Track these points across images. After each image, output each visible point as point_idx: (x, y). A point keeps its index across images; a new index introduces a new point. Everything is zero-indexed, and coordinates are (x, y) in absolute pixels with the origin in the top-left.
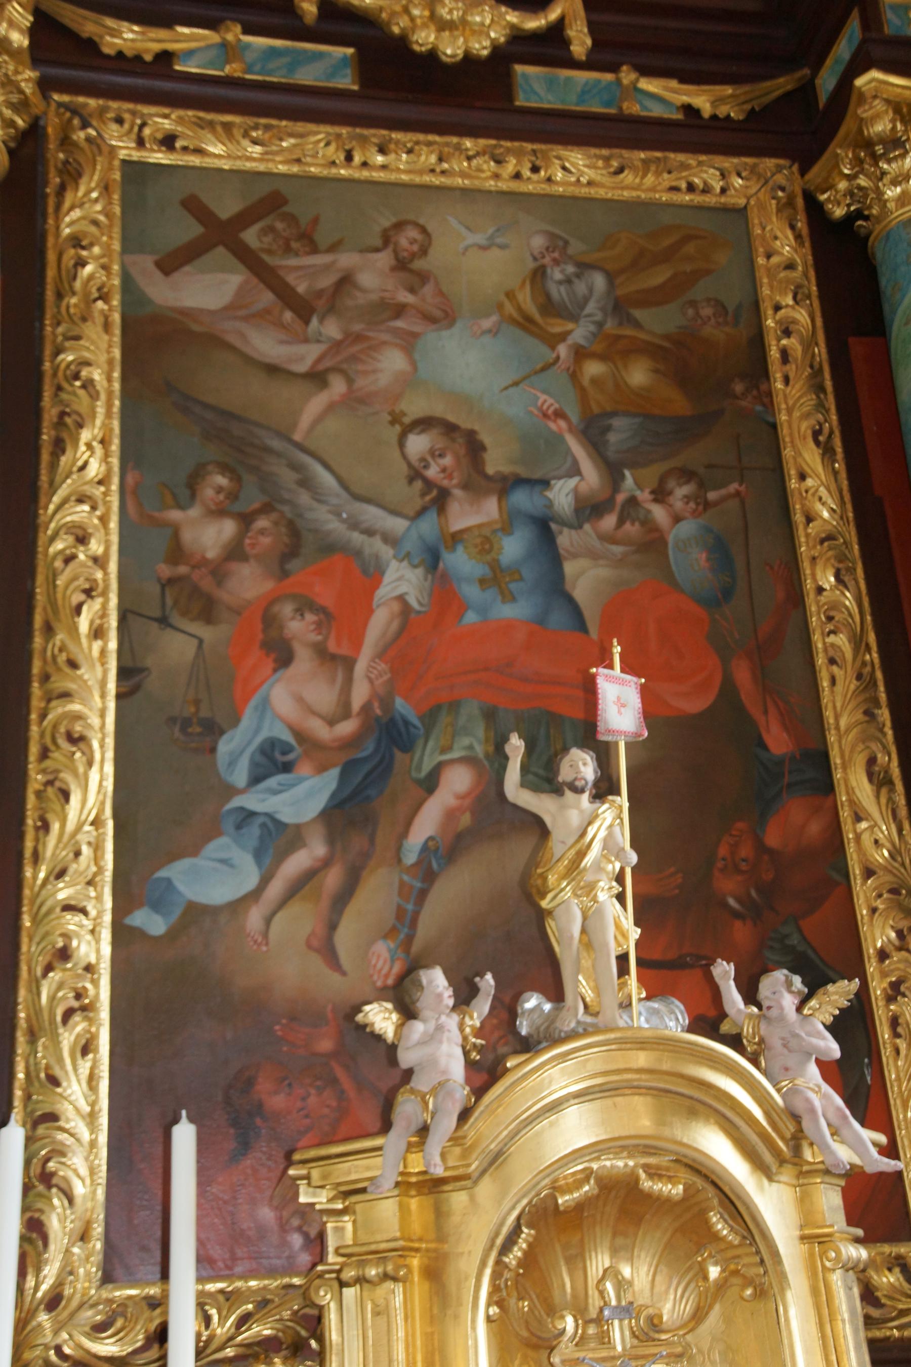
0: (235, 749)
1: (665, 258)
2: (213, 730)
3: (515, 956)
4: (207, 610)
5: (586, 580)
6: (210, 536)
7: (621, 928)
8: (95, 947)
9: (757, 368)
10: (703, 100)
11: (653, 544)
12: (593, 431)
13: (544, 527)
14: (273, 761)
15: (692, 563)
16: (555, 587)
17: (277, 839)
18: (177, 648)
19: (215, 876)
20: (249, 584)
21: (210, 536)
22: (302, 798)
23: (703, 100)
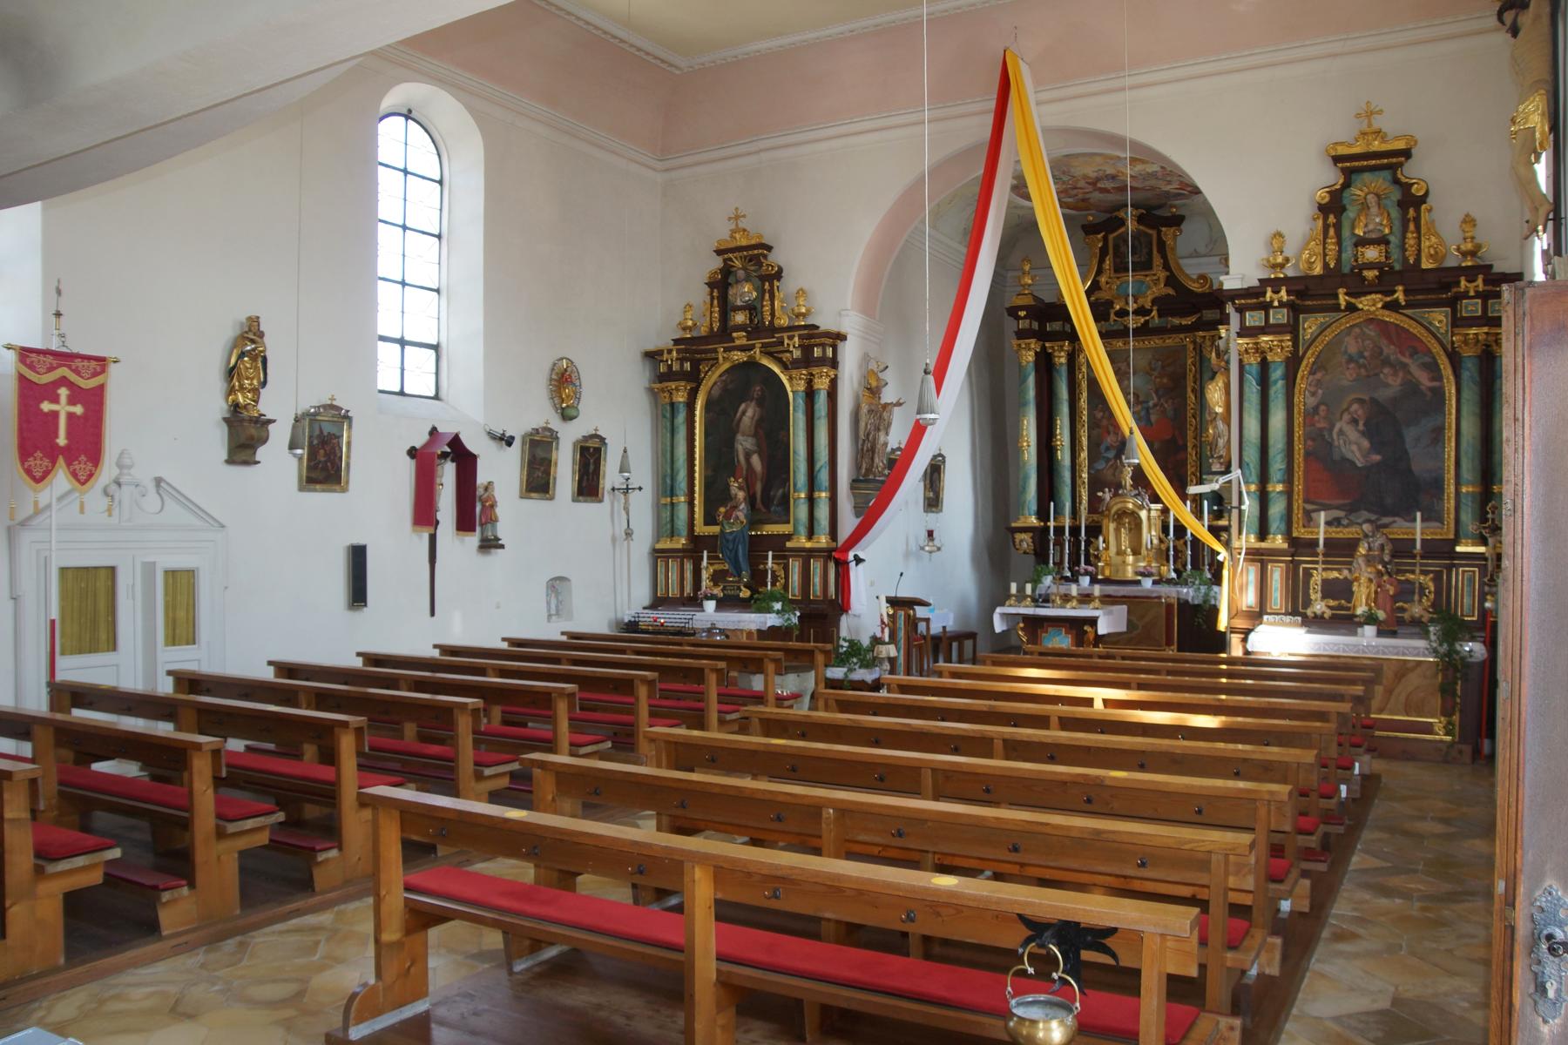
0: (1103, 447)
1: (1178, 353)
2: (1098, 445)
3: (1117, 486)
4: (1098, 426)
5: (1153, 418)
6: (1099, 415)
7: (1129, 482)
8: (1085, 475)
9: (1184, 377)
10: (1186, 321)
11: (1164, 411)
12: (1156, 392)
13: (1148, 410)
14: (1108, 449)
15: (1170, 413)
16: (1149, 420)
17: (1108, 460)
18: (1095, 432)
19: (1100, 465)
20: (1105, 422)
21: (1099, 415)
22: (1111, 454)
23: (1186, 321)
